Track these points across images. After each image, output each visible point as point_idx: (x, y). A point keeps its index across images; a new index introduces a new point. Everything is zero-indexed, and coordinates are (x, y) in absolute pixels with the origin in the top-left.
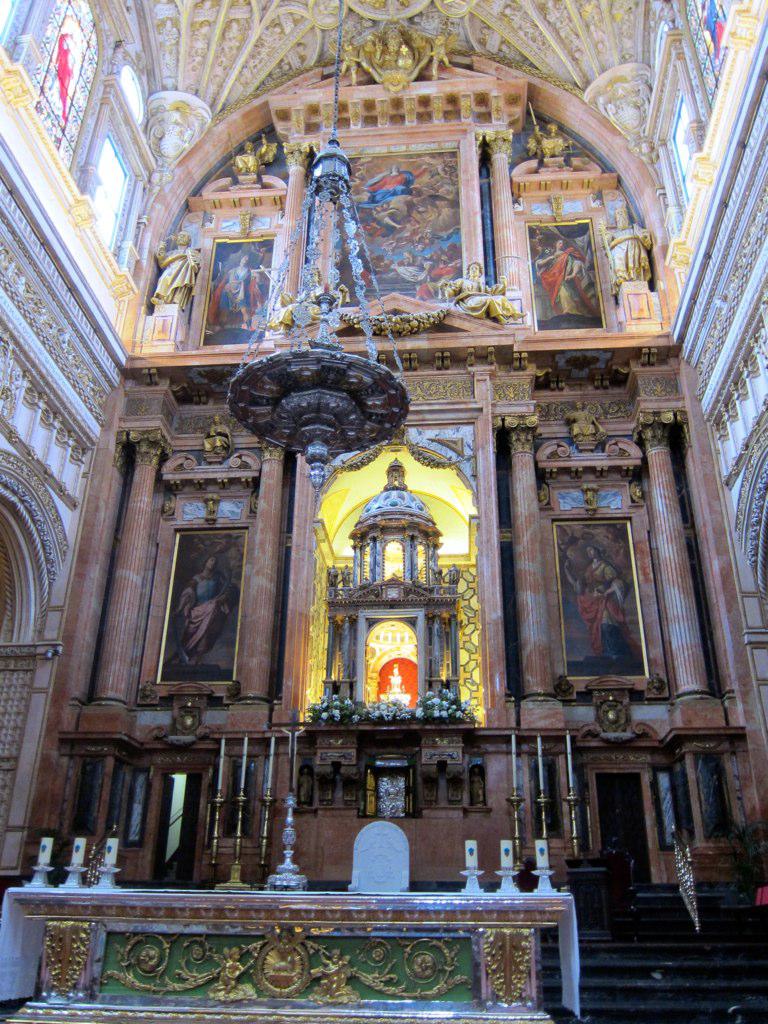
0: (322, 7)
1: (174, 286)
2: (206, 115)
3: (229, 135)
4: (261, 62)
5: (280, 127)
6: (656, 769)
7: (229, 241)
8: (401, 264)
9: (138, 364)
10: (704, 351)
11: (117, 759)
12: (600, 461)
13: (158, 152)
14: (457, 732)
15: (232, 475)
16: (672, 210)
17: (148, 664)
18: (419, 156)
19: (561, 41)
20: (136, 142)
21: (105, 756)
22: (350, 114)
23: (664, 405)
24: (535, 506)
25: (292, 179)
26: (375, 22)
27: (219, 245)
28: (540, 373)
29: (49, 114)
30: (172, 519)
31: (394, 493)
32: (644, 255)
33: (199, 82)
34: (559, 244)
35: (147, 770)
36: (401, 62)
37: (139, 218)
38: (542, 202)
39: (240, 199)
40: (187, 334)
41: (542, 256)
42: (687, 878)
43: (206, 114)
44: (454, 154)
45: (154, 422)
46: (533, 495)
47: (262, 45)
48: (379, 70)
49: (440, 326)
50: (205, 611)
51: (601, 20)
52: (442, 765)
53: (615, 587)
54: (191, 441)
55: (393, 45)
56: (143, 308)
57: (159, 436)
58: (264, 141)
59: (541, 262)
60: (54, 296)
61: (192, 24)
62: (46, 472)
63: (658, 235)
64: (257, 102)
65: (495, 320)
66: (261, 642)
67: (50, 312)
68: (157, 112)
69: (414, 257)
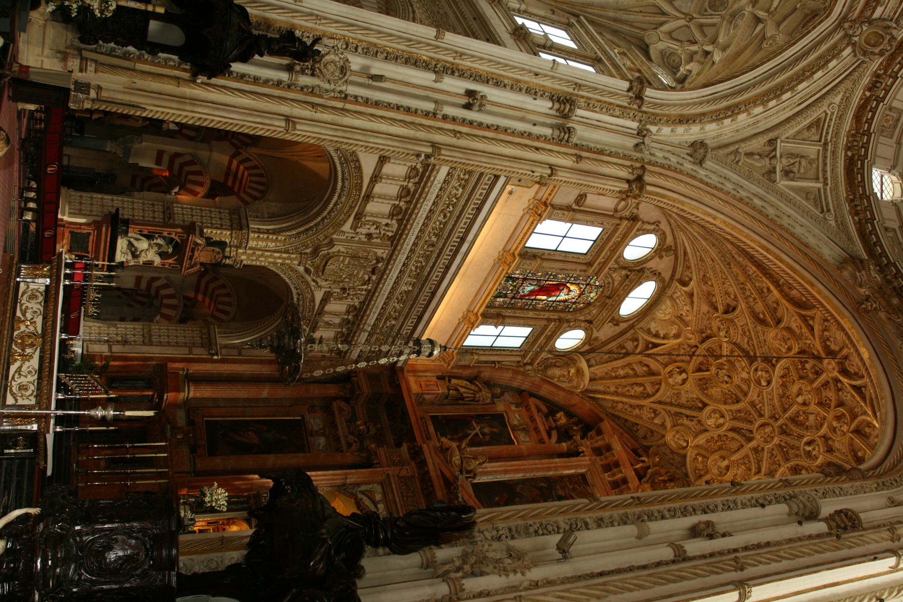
0: (677, 436)
1: (459, 388)
2: (582, 387)
3: (576, 404)
4: (631, 412)
5: (593, 433)
7: (506, 420)
11: (153, 396)
13: (547, 365)
15: (342, 438)
20: (542, 348)
22: (615, 470)
27: (502, 415)
29: (515, 286)
30: (309, 413)
33: (601, 379)
37: (498, 362)
39: (535, 420)
40: (433, 403)
45: (366, 389)
47: (640, 409)
48: (650, 481)
57: (357, 393)
58: (580, 426)
60: (410, 309)
62: (314, 328)
64: (602, 415)
67: (403, 308)
68: (571, 360)
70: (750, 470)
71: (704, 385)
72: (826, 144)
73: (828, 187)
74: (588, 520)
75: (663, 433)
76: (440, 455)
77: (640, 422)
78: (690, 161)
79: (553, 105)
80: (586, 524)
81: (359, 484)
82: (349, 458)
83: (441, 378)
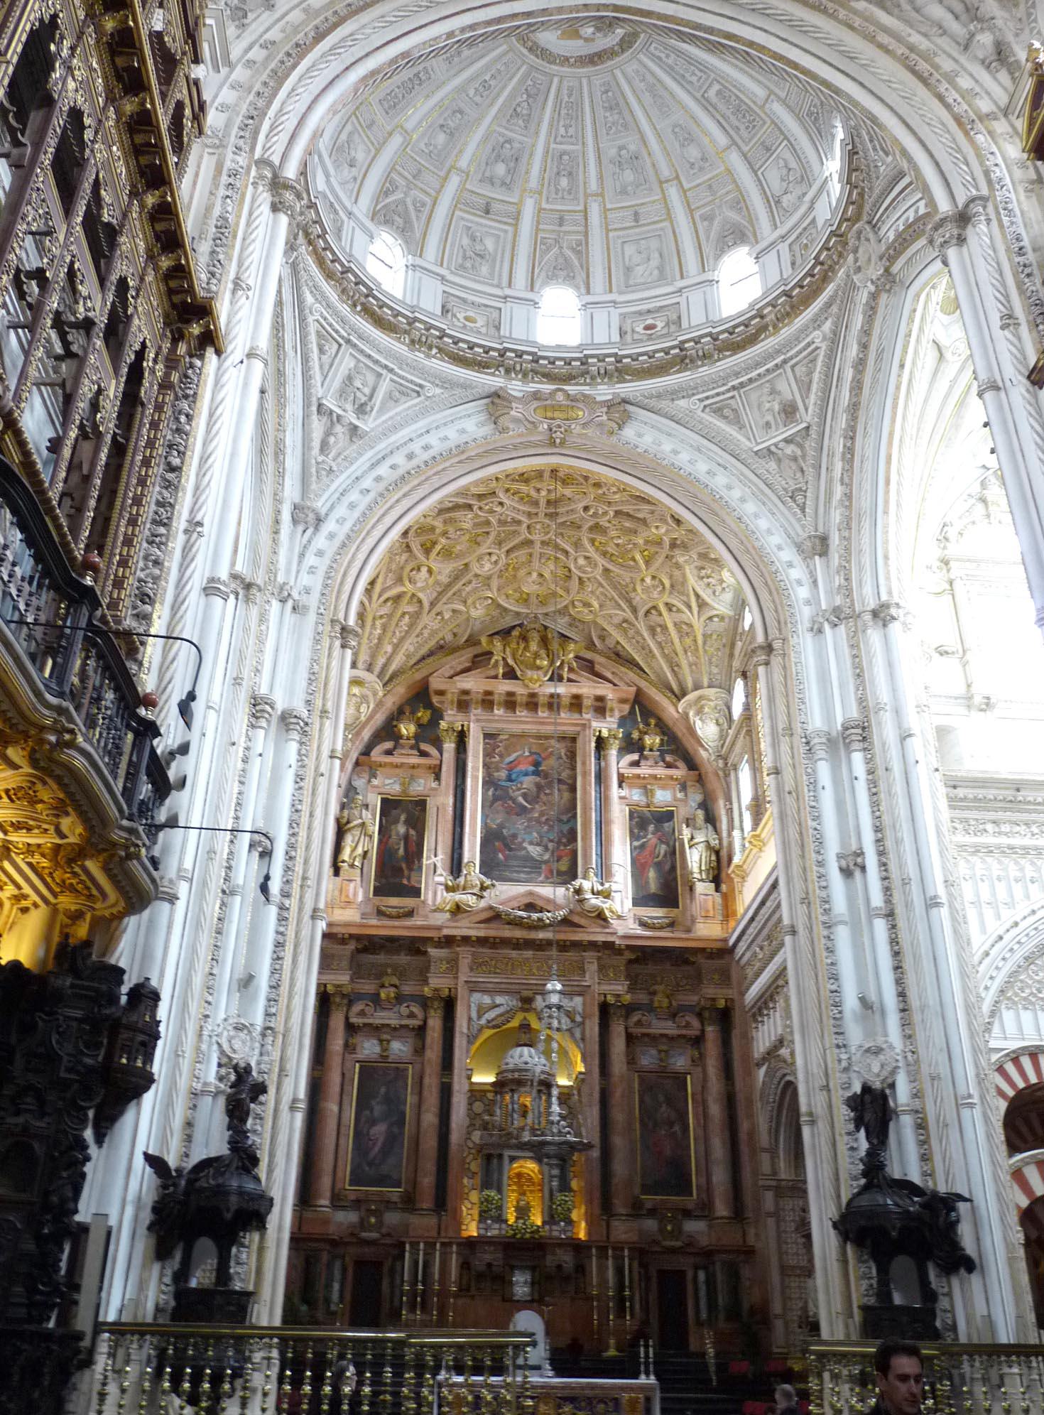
5: (435, 700)
6: (696, 1268)
8: (531, 843)
9: (335, 930)
10: (748, 963)
12: (669, 1028)
14: (569, 1245)
15: (403, 1022)
16: (736, 833)
17: (340, 1174)
18: (547, 738)
19: (665, 656)
21: (321, 1250)
22: (496, 698)
23: (719, 991)
24: (625, 1067)
25: (446, 755)
26: (518, 614)
28: (633, 957)
31: (526, 1049)
32: (714, 858)
34: (651, 828)
35: (343, 1257)
36: (538, 662)
38: (640, 788)
39: (402, 764)
41: (638, 839)
42: (711, 1351)
43: (378, 687)
44: (574, 740)
45: (343, 978)
46: (624, 1059)
49: (566, 921)
50: (379, 1130)
51: (697, 650)
52: (559, 1267)
53: (677, 1128)
54: (368, 987)
55: (534, 646)
56: (331, 871)
59: (636, 844)
61: (374, 619)
63: (725, 843)
64: (418, 676)
65: (605, 920)
66: (429, 1166)
69: (541, 837)
70: (556, 558)
71: (447, 554)
72: (348, 341)
73: (397, 370)
74: (829, 961)
75: (465, 616)
76: (460, 916)
77: (441, 635)
78: (314, 534)
79: (261, 727)
80: (832, 964)
81: (470, 1019)
82: (435, 1023)
83: (337, 871)
